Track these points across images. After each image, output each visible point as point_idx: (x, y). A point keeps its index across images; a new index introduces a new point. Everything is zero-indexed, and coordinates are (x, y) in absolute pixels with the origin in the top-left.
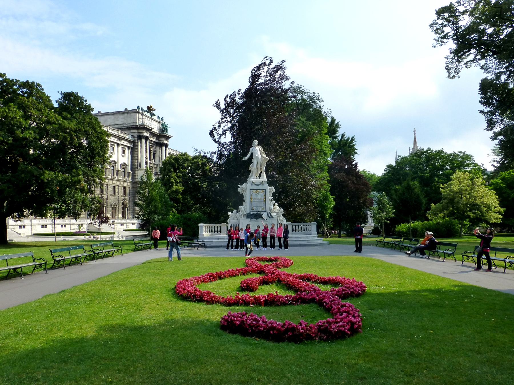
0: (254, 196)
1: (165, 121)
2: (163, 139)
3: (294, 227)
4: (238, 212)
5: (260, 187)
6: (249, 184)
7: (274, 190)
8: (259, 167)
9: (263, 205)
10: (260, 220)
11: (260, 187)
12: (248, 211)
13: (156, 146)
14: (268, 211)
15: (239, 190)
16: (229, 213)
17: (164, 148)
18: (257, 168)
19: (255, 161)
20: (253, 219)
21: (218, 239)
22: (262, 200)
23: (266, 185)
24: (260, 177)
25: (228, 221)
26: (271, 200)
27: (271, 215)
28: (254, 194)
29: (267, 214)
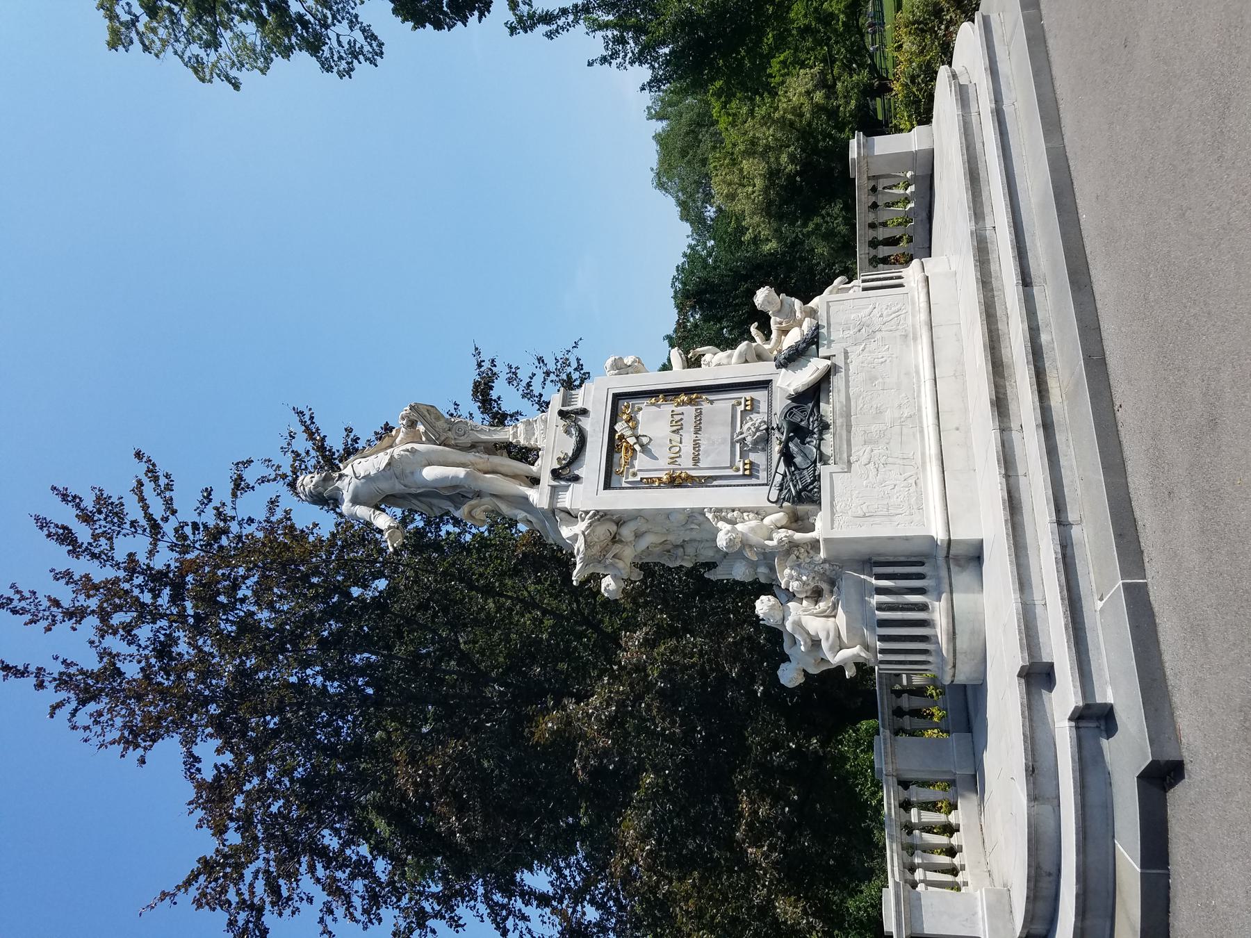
12: (756, 496)
20: (827, 449)
21: (1038, 677)
22: (690, 411)
28: (641, 461)
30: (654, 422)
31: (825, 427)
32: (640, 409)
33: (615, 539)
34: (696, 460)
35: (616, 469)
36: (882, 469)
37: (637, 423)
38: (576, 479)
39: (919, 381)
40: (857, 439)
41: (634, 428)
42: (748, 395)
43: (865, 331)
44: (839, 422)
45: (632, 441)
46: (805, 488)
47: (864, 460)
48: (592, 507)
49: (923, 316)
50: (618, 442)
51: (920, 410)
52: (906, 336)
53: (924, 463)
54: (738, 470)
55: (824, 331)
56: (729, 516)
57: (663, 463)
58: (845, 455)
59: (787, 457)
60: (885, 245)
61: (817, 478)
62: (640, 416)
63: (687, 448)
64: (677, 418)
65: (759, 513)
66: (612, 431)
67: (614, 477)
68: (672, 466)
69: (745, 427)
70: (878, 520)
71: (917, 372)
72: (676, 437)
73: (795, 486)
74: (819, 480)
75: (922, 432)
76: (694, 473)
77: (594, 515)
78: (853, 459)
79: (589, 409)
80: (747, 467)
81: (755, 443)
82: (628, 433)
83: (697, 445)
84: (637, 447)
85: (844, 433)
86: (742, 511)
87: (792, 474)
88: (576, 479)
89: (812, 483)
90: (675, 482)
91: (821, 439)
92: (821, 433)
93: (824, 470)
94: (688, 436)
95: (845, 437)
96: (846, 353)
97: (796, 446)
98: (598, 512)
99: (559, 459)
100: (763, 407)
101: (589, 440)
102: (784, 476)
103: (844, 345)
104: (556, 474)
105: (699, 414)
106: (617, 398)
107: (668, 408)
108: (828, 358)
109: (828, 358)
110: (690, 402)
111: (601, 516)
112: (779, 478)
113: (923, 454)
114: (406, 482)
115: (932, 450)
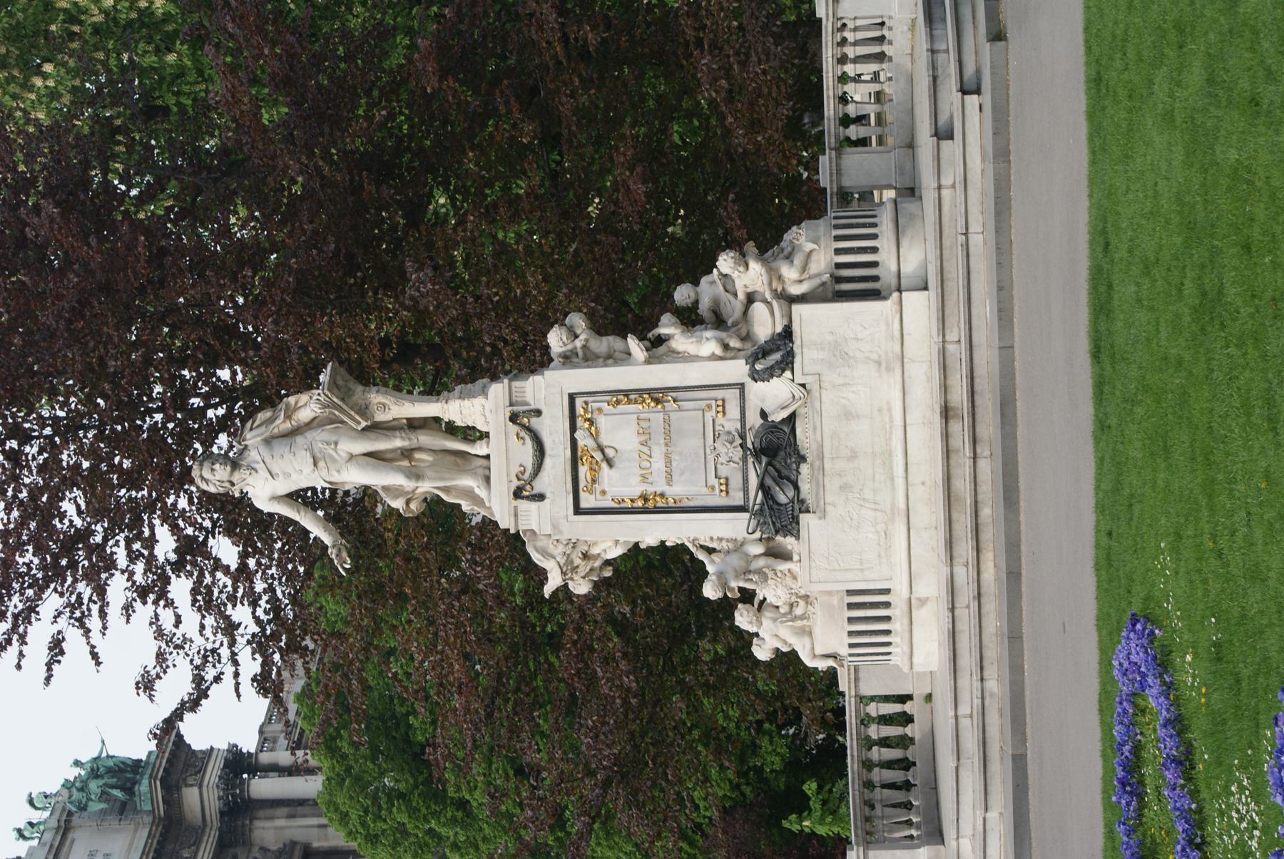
0: (619, 483)
1: (55, 774)
2: (191, 796)
4: (747, 596)
5: (553, 428)
6: (531, 520)
8: (398, 443)
10: (805, 436)
11: (553, 428)
13: (248, 843)
15: (581, 587)
16: (762, 653)
17: (262, 787)
19: (354, 477)
20: (805, 487)
23: (546, 390)
24: (470, 434)
25: (822, 665)
27: (763, 352)
30: (619, 430)
31: (803, 459)
33: (585, 556)
34: (669, 480)
35: (582, 484)
37: (597, 432)
38: (541, 497)
39: (891, 421)
40: (832, 484)
41: (595, 438)
42: (719, 394)
43: (839, 353)
44: (817, 463)
49: (897, 349)
51: (890, 455)
52: (879, 364)
53: (893, 513)
54: (713, 488)
62: (602, 421)
63: (658, 464)
64: (644, 424)
65: (739, 546)
66: (574, 443)
67: (583, 495)
71: (890, 410)
72: (645, 449)
73: (774, 523)
74: (798, 523)
75: (892, 479)
78: (829, 508)
80: (723, 488)
82: (590, 443)
83: (668, 461)
84: (604, 465)
85: (821, 477)
86: (721, 539)
87: (771, 508)
88: (541, 497)
90: (648, 506)
92: (798, 467)
93: (804, 518)
94: (658, 452)
97: (775, 481)
100: (733, 411)
101: (548, 451)
102: (762, 504)
103: (817, 368)
104: (518, 494)
105: (667, 422)
108: (803, 386)
109: (803, 386)
112: (756, 507)
113: (893, 504)
114: (332, 480)
115: (902, 505)
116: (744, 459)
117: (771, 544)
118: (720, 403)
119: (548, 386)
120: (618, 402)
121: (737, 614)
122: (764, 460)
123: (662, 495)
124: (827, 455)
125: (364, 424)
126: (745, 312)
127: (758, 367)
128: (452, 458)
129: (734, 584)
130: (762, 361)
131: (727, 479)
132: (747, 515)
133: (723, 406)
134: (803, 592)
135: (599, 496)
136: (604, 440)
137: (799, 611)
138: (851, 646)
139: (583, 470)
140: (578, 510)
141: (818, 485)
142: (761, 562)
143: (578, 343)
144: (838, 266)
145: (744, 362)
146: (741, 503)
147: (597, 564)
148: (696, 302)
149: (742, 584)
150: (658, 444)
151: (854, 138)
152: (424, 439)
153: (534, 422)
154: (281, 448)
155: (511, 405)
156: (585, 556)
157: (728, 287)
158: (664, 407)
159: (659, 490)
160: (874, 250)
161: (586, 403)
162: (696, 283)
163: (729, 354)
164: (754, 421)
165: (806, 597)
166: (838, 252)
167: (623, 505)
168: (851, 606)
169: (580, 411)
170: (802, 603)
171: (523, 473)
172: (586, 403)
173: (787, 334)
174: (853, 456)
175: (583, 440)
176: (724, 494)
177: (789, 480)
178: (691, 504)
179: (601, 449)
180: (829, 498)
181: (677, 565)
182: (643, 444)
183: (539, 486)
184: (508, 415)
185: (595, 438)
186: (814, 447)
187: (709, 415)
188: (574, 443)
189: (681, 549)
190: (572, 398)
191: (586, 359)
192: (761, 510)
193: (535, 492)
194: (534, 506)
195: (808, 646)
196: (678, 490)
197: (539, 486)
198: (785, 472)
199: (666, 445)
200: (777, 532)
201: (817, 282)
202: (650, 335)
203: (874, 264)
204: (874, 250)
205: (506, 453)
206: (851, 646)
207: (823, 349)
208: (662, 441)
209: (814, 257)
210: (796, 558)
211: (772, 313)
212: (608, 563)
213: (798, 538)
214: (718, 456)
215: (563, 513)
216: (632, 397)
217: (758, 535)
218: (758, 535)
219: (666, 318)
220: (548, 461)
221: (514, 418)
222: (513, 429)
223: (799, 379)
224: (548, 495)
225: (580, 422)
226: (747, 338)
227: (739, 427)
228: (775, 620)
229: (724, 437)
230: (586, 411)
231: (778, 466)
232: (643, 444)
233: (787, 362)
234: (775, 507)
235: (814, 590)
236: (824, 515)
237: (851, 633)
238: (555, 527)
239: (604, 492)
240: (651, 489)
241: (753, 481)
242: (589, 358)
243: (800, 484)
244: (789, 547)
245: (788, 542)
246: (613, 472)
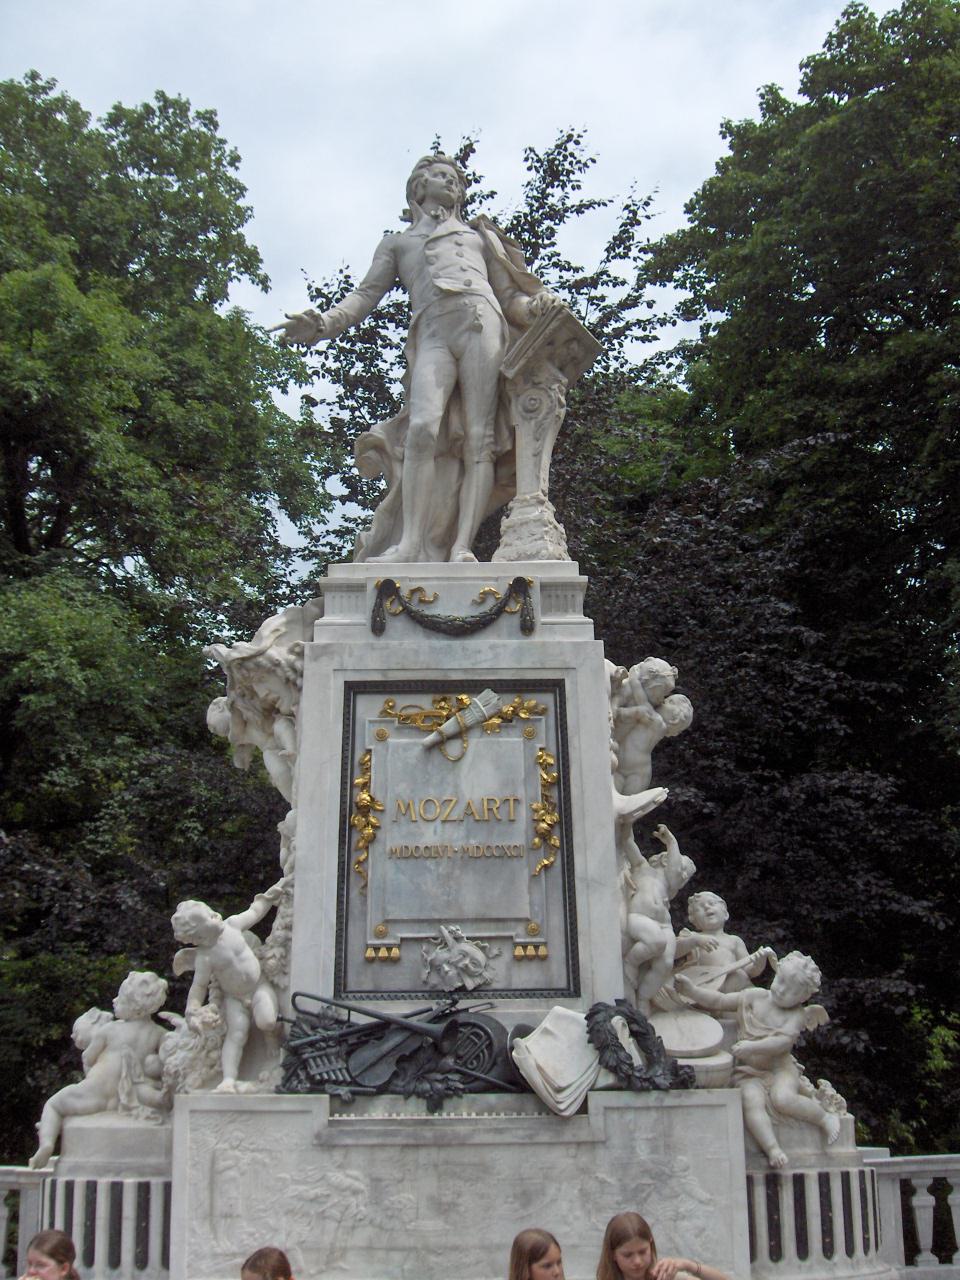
3: (924, 1202)
5: (497, 652)
7: (681, 708)
8: (478, 429)
9: (525, 897)
11: (497, 652)
12: (311, 972)
14: (606, 979)
16: (88, 1026)
18: (451, 448)
20: (379, 1110)
24: (486, 543)
26: (643, 833)
27: (643, 1036)
28: (406, 746)
29: (596, 1018)
31: (435, 1105)
32: (530, 737)
34: (405, 855)
35: (402, 701)
36: (314, 1209)
37: (493, 728)
38: (378, 628)
41: (482, 725)
42: (557, 951)
44: (428, 1133)
45: (448, 727)
46: (305, 1065)
47: (337, 1177)
48: (309, 667)
50: (453, 697)
54: (380, 935)
55: (652, 1098)
56: (277, 923)
57: (403, 789)
58: (349, 1141)
59: (382, 1027)
60: (936, 1210)
61: (317, 1086)
62: (512, 741)
63: (429, 836)
65: (273, 977)
66: (474, 687)
68: (390, 807)
69: (468, 947)
70: (204, 1195)
73: (312, 1044)
74: (310, 1091)
76: (376, 849)
77: (295, 670)
78: (338, 1155)
79: (537, 638)
80: (383, 953)
81: (435, 967)
82: (469, 718)
83: (432, 853)
84: (431, 738)
85: (399, 1140)
86: (286, 943)
87: (341, 1040)
89: (310, 1078)
91: (407, 1095)
92: (420, 1095)
94: (456, 837)
95: (389, 1140)
96: (593, 1144)
98: (302, 676)
99: (419, 589)
100: (526, 977)
101: (457, 644)
103: (616, 1140)
104: (387, 589)
105: (504, 855)
106: (556, 687)
107: (530, 794)
108: (584, 1109)
109: (584, 1109)
110: (538, 833)
111: (293, 682)
112: (344, 1014)
116: (435, 994)
117: (271, 1040)
118: (542, 951)
119: (576, 645)
120: (546, 767)
121: (148, 975)
122: (439, 1028)
123: (372, 839)
124: (443, 1154)
125: (510, 374)
126: (700, 1007)
127: (618, 1021)
128: (444, 521)
129: (201, 964)
130: (627, 1032)
131: (395, 961)
132: (328, 992)
133: (536, 958)
134: (179, 1098)
135: (376, 728)
136: (475, 741)
137: (147, 1089)
138: (70, 1187)
139: (425, 702)
140: (353, 690)
141: (386, 1134)
142: (239, 1020)
143: (644, 708)
144: (799, 1181)
145: (621, 996)
146: (352, 986)
147: (255, 736)
148: (693, 928)
149: (197, 977)
150: (468, 837)
151: (916, 1201)
152: (480, 473)
153: (509, 622)
154: (477, 261)
155: (544, 587)
156: (271, 712)
157: (734, 980)
158: (534, 848)
159: (380, 834)
160: (828, 1250)
161: (544, 712)
162: (729, 928)
163: (632, 972)
164: (508, 1013)
165: (165, 1107)
166: (824, 1180)
167: (357, 770)
168: (144, 1189)
169: (532, 700)
170: (158, 1095)
171: (421, 601)
172: (544, 712)
173: (683, 1080)
174: (443, 1208)
175: (483, 703)
176: (370, 953)
177: (395, 1075)
178: (354, 893)
179: (460, 734)
180: (358, 1158)
181: (244, 866)
182: (469, 812)
183: (397, 626)
184: (528, 576)
185: (482, 725)
186: (462, 1129)
187: (519, 933)
188: (474, 687)
189: (276, 873)
190: (556, 687)
191: (618, 720)
192: (339, 1022)
193: (387, 615)
194: (363, 618)
195: (79, 1104)
196: (380, 868)
197: (397, 626)
198: (411, 1070)
199: (465, 851)
200: (295, 1052)
201: (769, 1137)
202: (663, 827)
203: (803, 1251)
204: (828, 1250)
205: (458, 582)
206: (70, 1187)
207: (654, 1150)
208: (473, 842)
209: (811, 1137)
210: (244, 1086)
211: (708, 1053)
212: (257, 759)
213: (278, 1091)
214: (445, 944)
215: (349, 663)
216: (554, 794)
217: (291, 1014)
218: (291, 1014)
219: (686, 865)
220: (440, 643)
221: (520, 587)
222: (501, 590)
223: (597, 1101)
224: (382, 641)
225: (508, 697)
226: (656, 1009)
227: (495, 986)
228: (133, 1044)
229: (480, 956)
230: (531, 711)
231: (422, 1056)
232: (469, 812)
233: (626, 1080)
234: (344, 1048)
235: (181, 1121)
236: (325, 1143)
237: (91, 1187)
238: (325, 650)
239: (381, 738)
240: (386, 821)
241: (396, 1010)
242: (622, 728)
243: (386, 1098)
244: (264, 1074)
245: (273, 1072)
246: (417, 751)
